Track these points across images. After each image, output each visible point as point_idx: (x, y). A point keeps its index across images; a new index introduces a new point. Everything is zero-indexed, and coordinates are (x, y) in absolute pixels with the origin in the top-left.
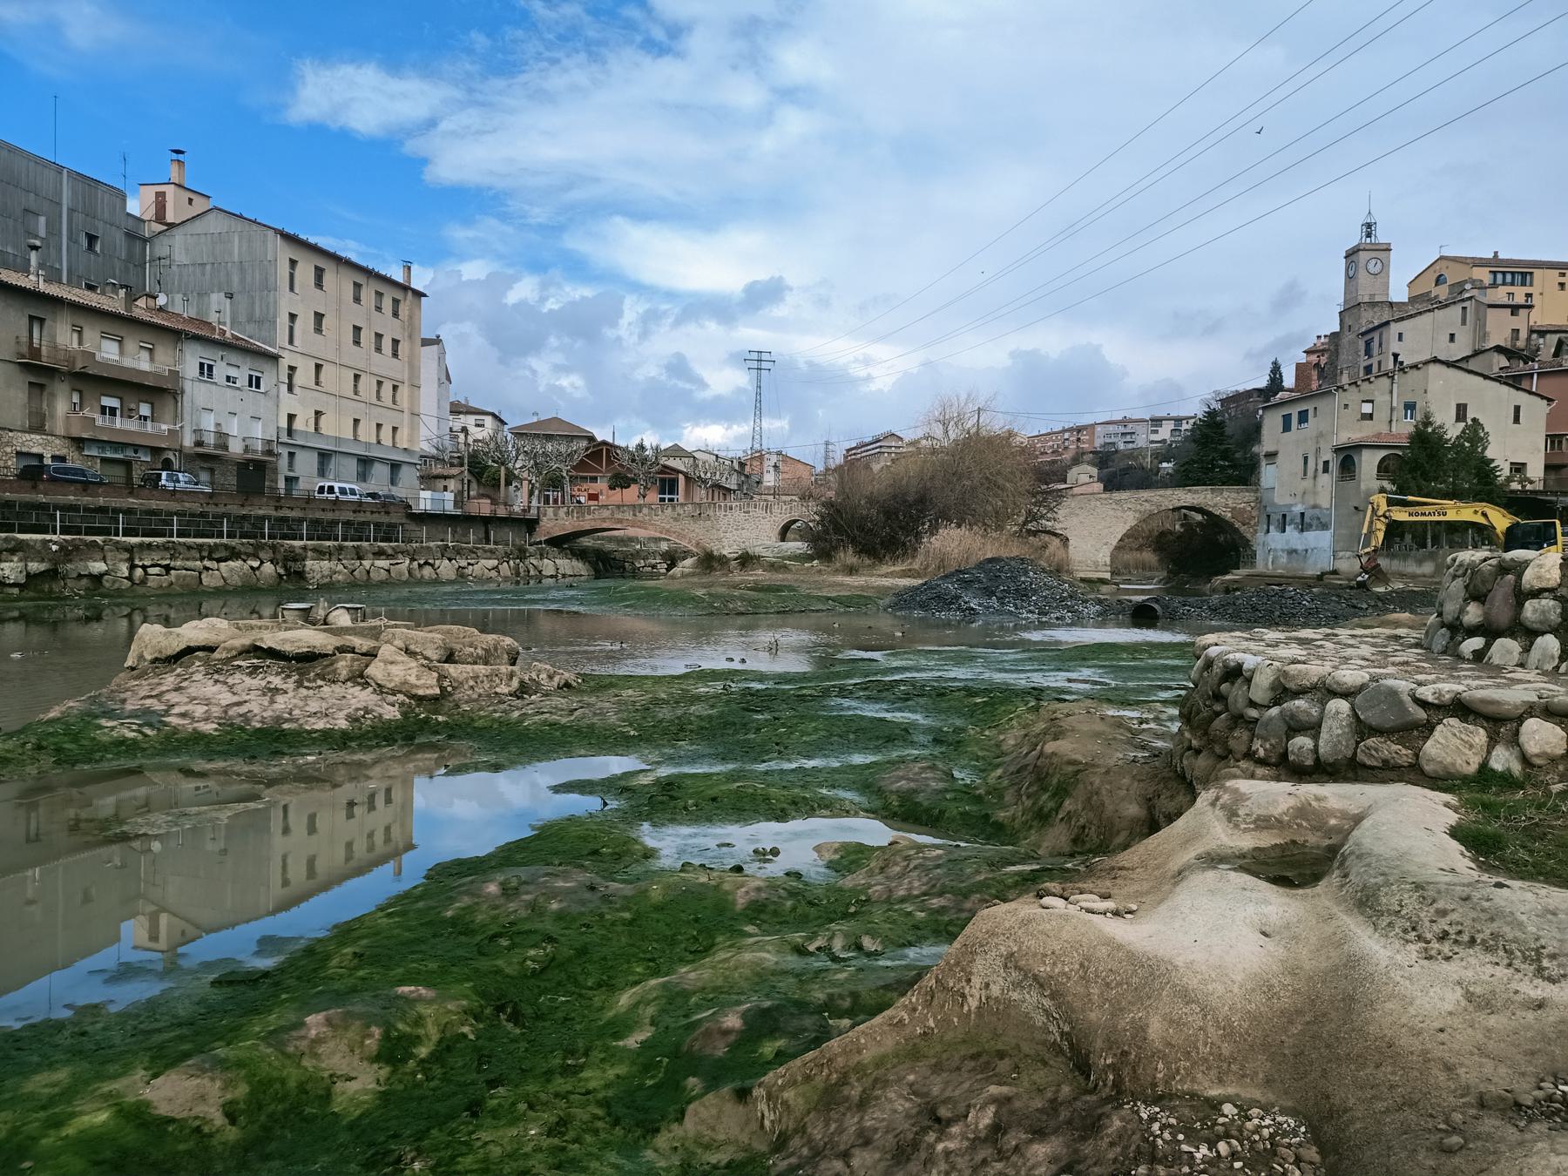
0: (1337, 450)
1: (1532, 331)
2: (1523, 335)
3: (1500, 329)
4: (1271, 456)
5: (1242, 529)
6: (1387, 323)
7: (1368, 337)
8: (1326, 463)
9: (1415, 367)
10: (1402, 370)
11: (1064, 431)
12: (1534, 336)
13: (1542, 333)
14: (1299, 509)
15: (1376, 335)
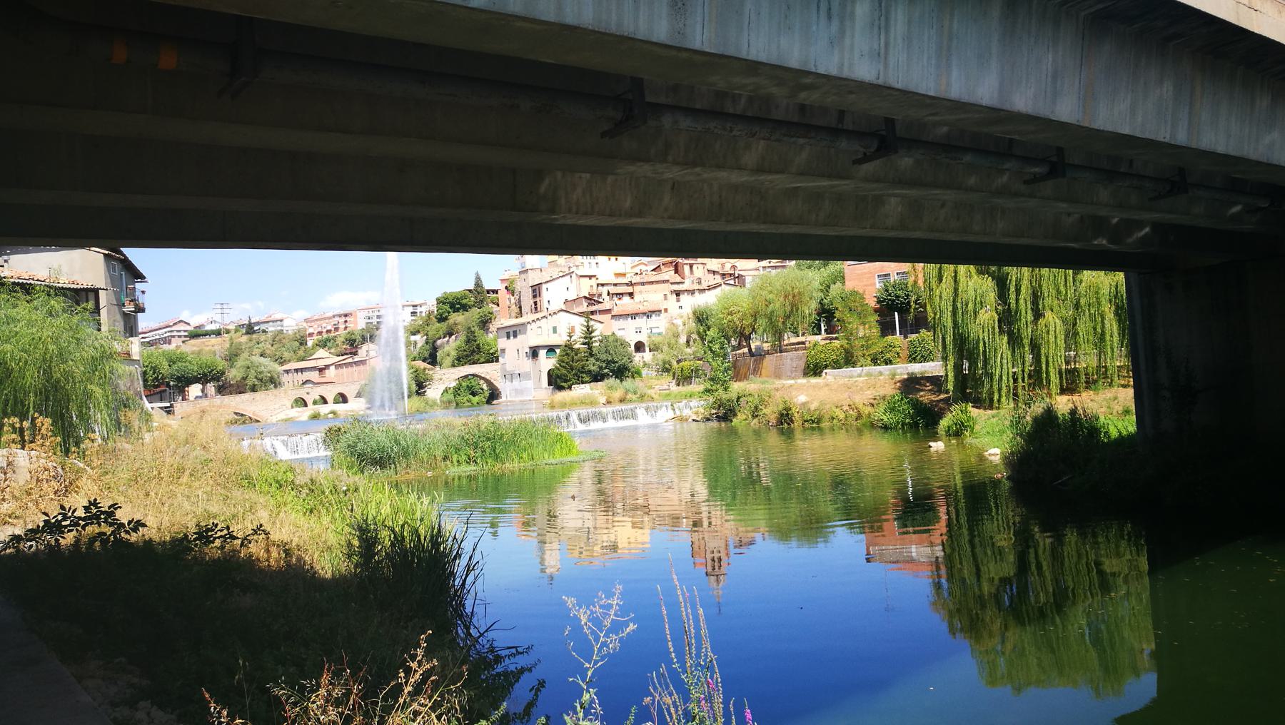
0: (530, 348)
1: (598, 285)
2: (595, 286)
3: (586, 288)
4: (503, 351)
5: (494, 382)
6: (541, 283)
7: (534, 288)
8: (527, 353)
9: (554, 313)
10: (550, 314)
11: (334, 316)
12: (600, 288)
13: (603, 285)
14: (517, 372)
15: (537, 287)
